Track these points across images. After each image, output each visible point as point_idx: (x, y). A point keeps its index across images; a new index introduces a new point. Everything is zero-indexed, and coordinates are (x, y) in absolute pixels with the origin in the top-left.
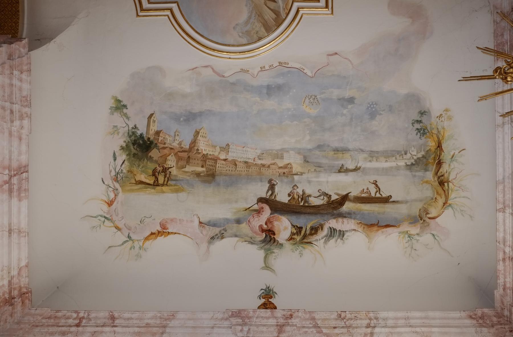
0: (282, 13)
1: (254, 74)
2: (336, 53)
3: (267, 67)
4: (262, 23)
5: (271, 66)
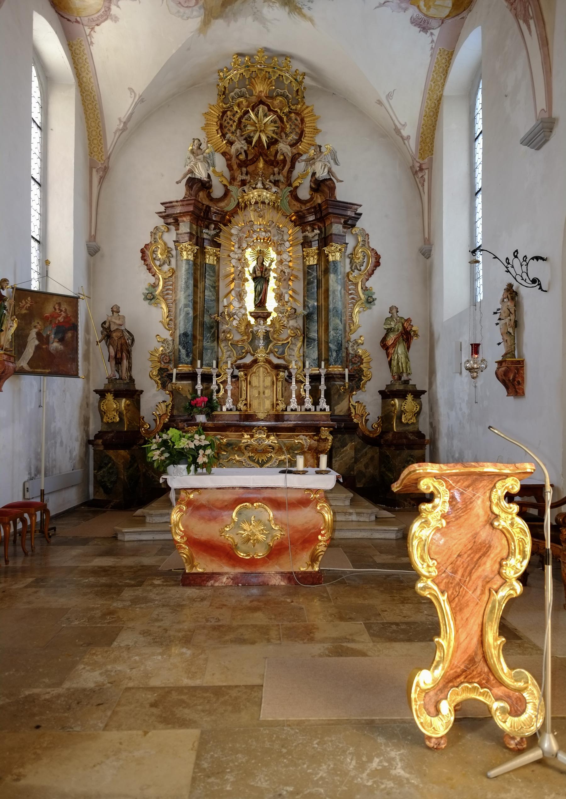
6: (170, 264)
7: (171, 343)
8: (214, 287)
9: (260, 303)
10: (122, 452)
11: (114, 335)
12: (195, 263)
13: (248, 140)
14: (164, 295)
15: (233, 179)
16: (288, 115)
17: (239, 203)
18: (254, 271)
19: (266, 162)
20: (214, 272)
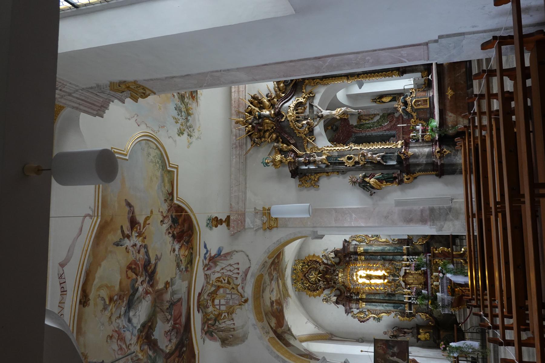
6: (365, 312)
7: (396, 312)
8: (374, 295)
9: (379, 277)
10: (441, 333)
11: (395, 334)
12: (366, 302)
13: (319, 281)
14: (377, 315)
15: (333, 287)
16: (309, 266)
17: (342, 285)
18: (368, 280)
19: (326, 275)
20: (368, 295)
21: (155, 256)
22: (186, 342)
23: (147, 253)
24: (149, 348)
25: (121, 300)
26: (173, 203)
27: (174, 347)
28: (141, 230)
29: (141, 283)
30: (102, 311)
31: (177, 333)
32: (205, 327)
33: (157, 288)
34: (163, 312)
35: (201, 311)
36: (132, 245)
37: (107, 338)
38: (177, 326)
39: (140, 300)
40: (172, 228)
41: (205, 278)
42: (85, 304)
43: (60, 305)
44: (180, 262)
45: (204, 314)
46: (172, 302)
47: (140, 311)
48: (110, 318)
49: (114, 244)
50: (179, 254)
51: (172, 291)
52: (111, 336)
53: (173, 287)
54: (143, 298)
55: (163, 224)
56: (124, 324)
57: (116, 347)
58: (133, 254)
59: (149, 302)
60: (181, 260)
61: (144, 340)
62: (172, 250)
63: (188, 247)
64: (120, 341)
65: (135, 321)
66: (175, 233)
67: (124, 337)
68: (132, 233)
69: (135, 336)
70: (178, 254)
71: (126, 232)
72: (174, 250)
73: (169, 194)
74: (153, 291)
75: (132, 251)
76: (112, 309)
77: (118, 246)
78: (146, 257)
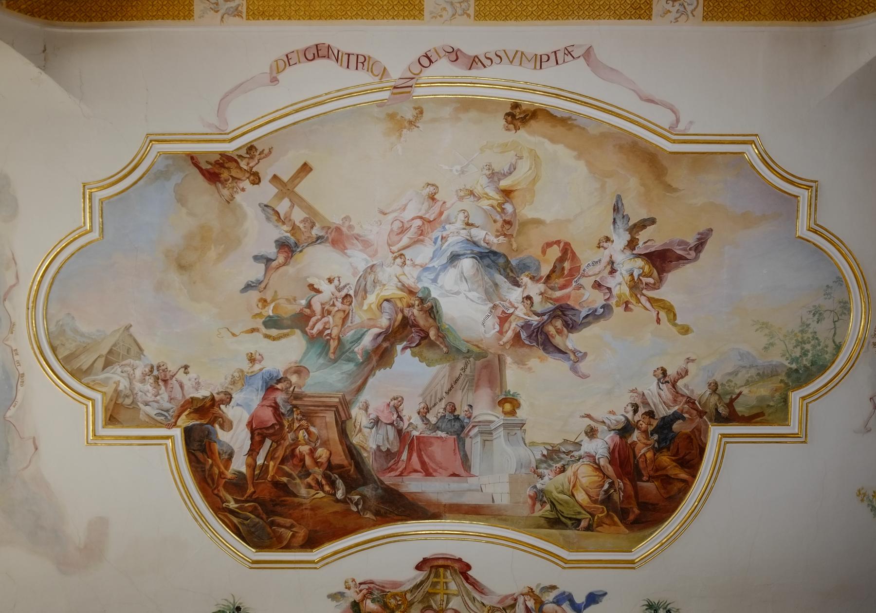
0: (90, 378)
1: (7, 340)
2: (36, 449)
3: (16, 358)
4: (75, 351)
5: (18, 363)
21: (583, 351)
22: (357, 497)
23: (594, 316)
24: (379, 335)
25: (503, 227)
26: (711, 420)
27: (356, 440)
28: (644, 292)
29: (529, 298)
30: (489, 167)
31: (389, 454)
32: (373, 600)
33: (509, 360)
34: (447, 393)
35: (420, 576)
36: (614, 258)
37: (433, 185)
38: (404, 456)
39: (492, 293)
40: (647, 418)
41: (506, 597)
42: (509, 118)
43: (519, 55)
44: (559, 465)
45: (409, 597)
46: (466, 431)
47: (467, 297)
48: (471, 193)
49: (619, 198)
50: (580, 458)
51: (493, 426)
52: (435, 197)
53: (501, 432)
54: (495, 307)
55: (659, 380)
56: (450, 240)
57: (408, 215)
58: (595, 263)
59: (482, 329)
60: (563, 470)
61: (402, 311)
62: (593, 424)
63: (595, 502)
64: (419, 227)
65: (449, 278)
66: (636, 436)
67: (422, 241)
68: (639, 256)
69: (419, 279)
70: (582, 452)
71: (643, 236)
72: (591, 433)
73: (732, 401)
74: (505, 343)
75: (600, 260)
76: (489, 198)
77: (614, 210)
78: (583, 314)
